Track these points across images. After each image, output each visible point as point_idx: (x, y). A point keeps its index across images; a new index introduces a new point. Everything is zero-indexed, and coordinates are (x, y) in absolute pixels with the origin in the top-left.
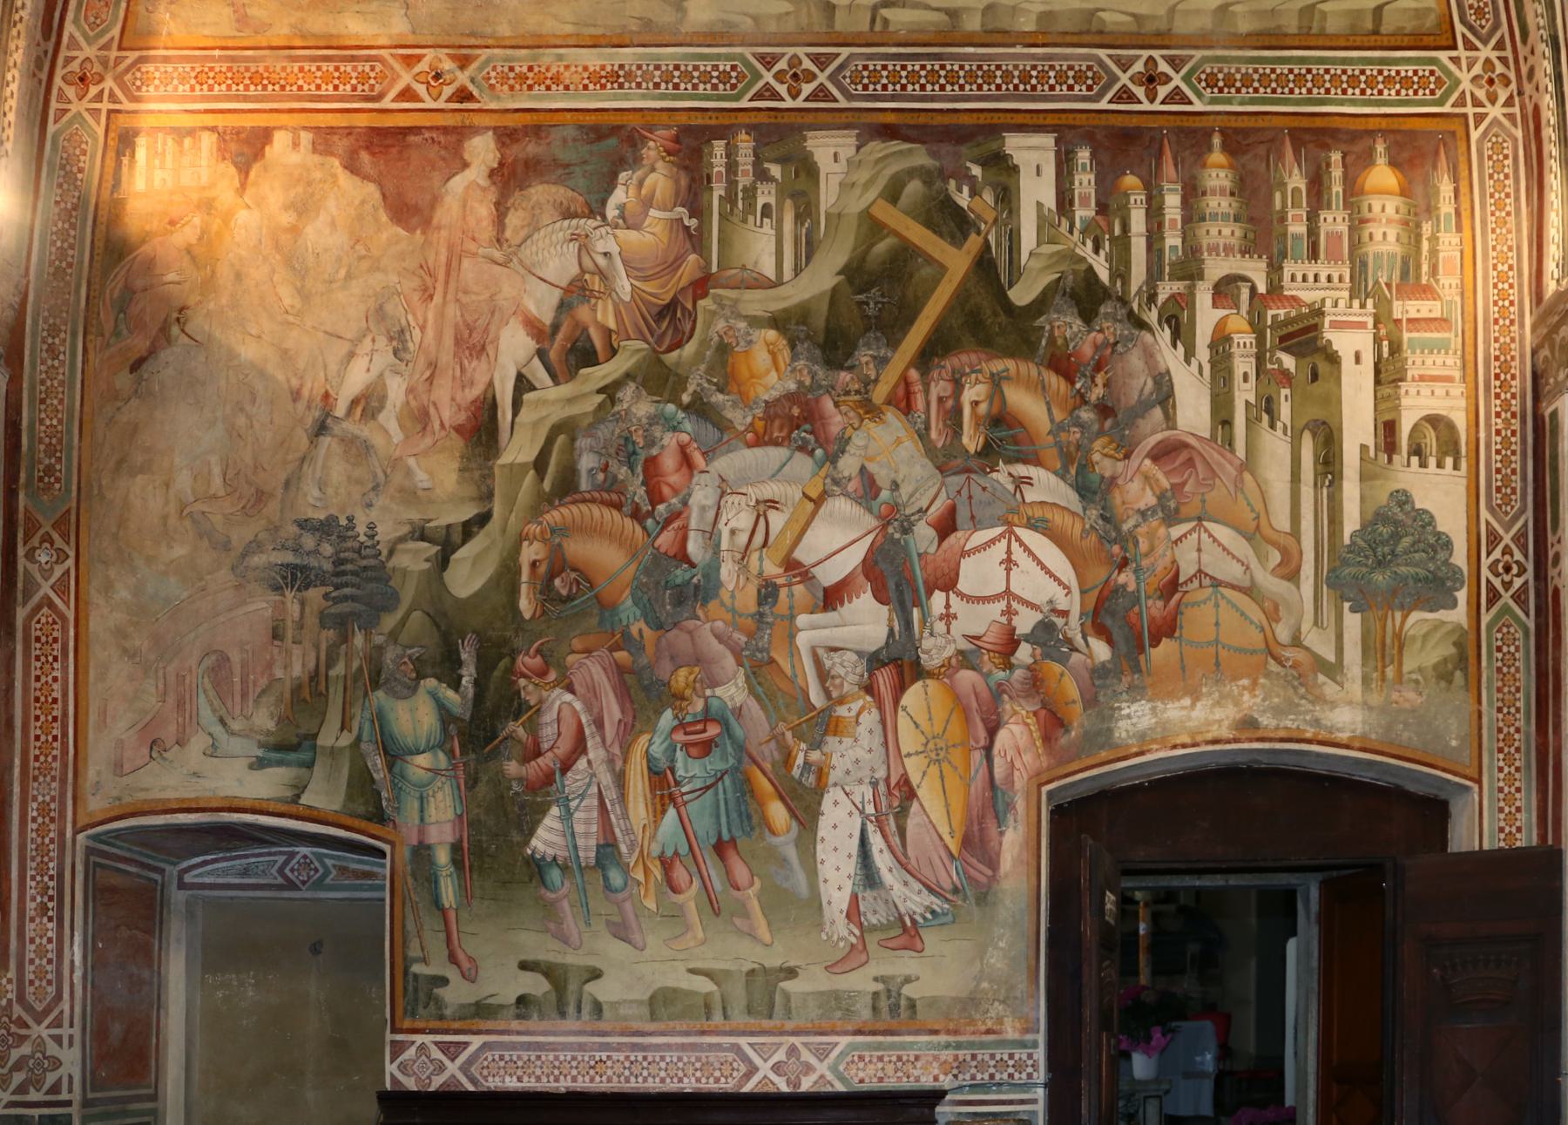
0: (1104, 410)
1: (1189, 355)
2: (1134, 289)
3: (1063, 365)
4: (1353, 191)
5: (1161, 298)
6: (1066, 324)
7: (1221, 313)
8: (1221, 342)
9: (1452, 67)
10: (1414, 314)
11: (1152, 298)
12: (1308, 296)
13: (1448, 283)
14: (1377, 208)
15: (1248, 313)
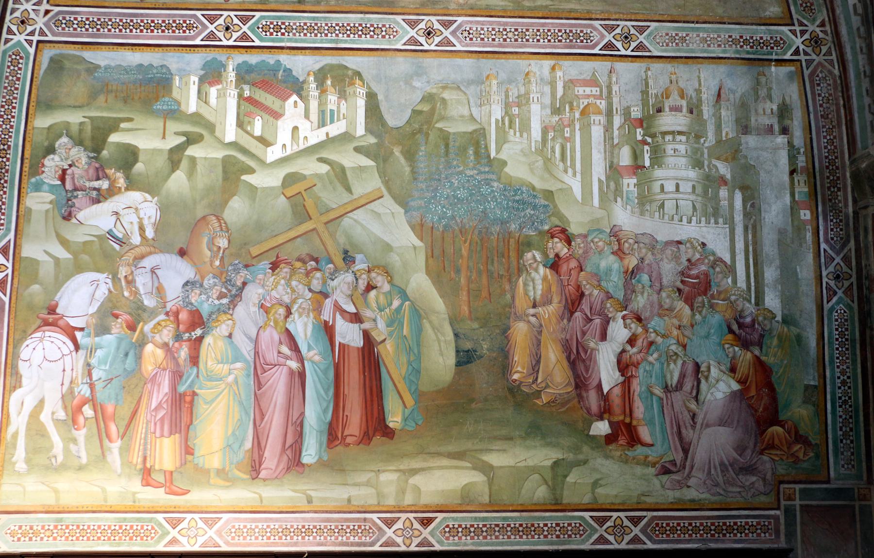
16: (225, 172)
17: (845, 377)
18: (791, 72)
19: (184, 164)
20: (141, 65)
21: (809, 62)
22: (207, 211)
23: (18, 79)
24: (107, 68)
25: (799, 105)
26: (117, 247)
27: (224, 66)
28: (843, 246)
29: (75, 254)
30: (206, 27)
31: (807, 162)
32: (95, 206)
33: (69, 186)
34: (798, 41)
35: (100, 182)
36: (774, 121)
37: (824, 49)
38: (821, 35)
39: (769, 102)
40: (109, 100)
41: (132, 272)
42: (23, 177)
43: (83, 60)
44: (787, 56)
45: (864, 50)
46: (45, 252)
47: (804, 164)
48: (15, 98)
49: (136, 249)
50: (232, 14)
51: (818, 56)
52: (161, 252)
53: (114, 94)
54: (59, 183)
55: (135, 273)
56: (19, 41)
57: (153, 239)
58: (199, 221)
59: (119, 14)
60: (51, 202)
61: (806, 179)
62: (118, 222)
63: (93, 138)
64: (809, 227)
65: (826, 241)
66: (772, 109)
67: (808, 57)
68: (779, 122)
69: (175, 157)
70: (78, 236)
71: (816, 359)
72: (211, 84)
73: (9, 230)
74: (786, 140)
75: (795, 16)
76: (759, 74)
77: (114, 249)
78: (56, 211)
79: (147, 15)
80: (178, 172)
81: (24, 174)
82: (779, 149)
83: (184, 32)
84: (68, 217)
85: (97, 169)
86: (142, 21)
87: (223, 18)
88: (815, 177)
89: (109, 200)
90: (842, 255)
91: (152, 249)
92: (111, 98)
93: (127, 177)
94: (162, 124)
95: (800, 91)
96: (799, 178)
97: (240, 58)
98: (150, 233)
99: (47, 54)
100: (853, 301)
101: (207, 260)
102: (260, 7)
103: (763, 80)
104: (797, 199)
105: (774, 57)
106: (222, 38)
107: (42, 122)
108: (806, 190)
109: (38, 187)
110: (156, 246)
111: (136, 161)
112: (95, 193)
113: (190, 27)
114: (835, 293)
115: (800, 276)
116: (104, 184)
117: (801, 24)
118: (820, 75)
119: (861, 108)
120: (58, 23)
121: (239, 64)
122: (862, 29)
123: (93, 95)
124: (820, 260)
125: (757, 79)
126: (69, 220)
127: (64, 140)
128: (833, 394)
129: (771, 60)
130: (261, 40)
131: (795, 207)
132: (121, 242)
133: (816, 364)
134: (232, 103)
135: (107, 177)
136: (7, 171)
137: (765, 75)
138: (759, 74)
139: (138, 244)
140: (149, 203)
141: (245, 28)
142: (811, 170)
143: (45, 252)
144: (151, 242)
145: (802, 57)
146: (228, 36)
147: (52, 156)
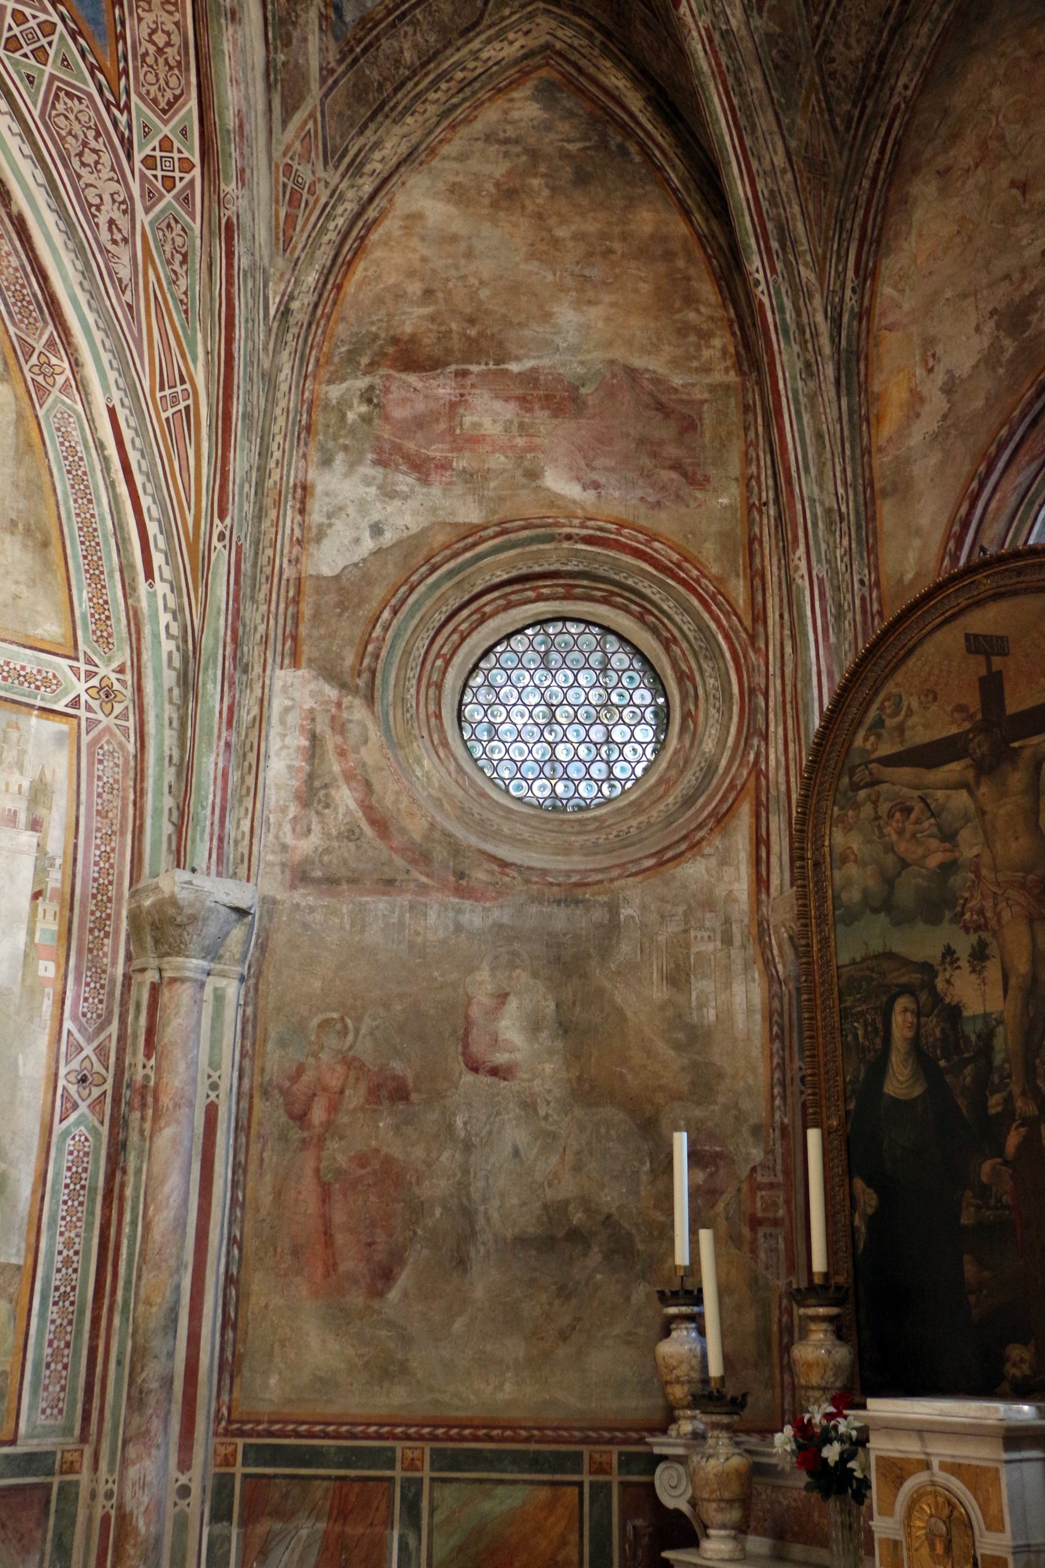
17: (71, 1253)
18: (61, 732)
21: (92, 723)
25: (65, 787)
28: (101, 1028)
31: (63, 882)
34: (80, 687)
36: (21, 807)
37: (118, 708)
38: (117, 686)
39: (17, 773)
44: (60, 707)
45: (175, 724)
47: (58, 885)
51: (107, 716)
61: (57, 909)
64: (49, 990)
65: (74, 1018)
66: (20, 786)
67: (91, 715)
68: (28, 809)
71: (26, 1221)
74: (35, 840)
75: (82, 647)
76: (9, 725)
82: (21, 853)
88: (72, 909)
90: (95, 1044)
95: (70, 765)
96: (47, 907)
100: (102, 1123)
103: (14, 735)
104: (37, 941)
105: (38, 703)
108: (55, 928)
114: (75, 1106)
115: (21, 1073)
117: (89, 661)
118: (106, 747)
119: (157, 812)
122: (176, 692)
124: (59, 1049)
125: (5, 732)
128: (47, 1280)
129: (32, 707)
131: (30, 955)
133: (25, 1227)
137: (18, 728)
138: (9, 725)
142: (68, 897)
145: (82, 713)
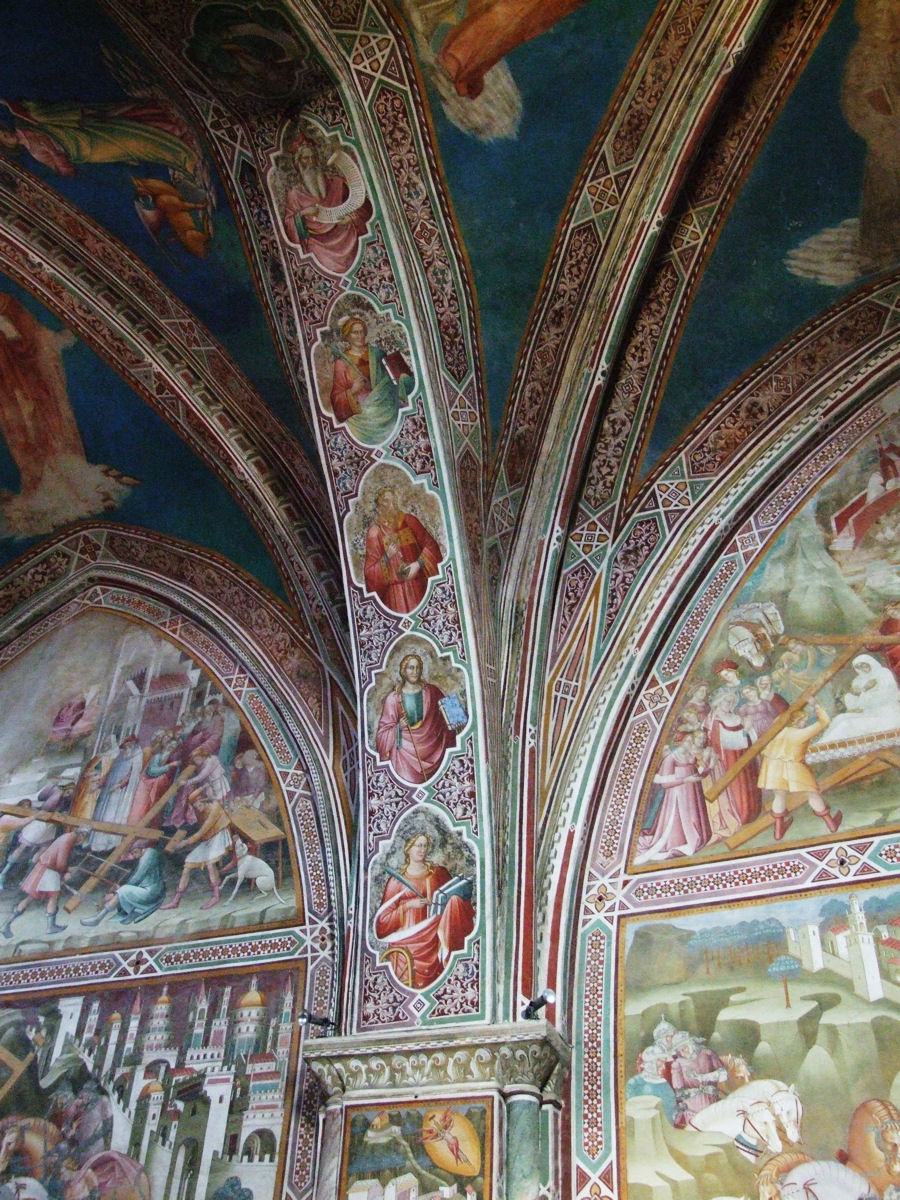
0: (73, 1142)
1: (126, 1105)
2: (104, 1073)
3: (57, 1119)
4: (234, 1005)
5: (117, 1076)
6: (66, 1098)
7: (148, 1081)
8: (145, 1097)
9: (301, 935)
10: (258, 1071)
11: (112, 1077)
12: (198, 1067)
13: (282, 1052)
14: (246, 1013)
15: (164, 1080)
16: (880, 1040)
19: (822, 1036)
20: (743, 924)
22: (867, 1096)
23: (601, 962)
24: (703, 933)
26: (752, 1158)
27: (848, 907)
29: (698, 1174)
30: (816, 866)
32: (714, 1105)
33: (677, 1083)
35: (716, 1073)
40: (712, 971)
41: (778, 1193)
42: (619, 1079)
43: (672, 929)
46: (658, 1174)
48: (600, 985)
49: (779, 1159)
50: (844, 845)
52: (813, 1159)
53: (716, 963)
54: (664, 1080)
55: (782, 1193)
56: (599, 921)
57: (799, 1143)
58: (857, 1110)
59: (708, 870)
60: (656, 1108)
62: (747, 1123)
63: (698, 1019)
69: (808, 1030)
70: (697, 1148)
72: (836, 931)
73: (609, 1149)
77: (749, 1162)
78: (664, 1116)
79: (740, 865)
80: (815, 1047)
81: (619, 1074)
83: (789, 876)
84: (681, 1124)
85: (709, 1058)
86: (736, 873)
87: (833, 852)
89: (730, 1096)
91: (801, 1157)
92: (713, 966)
93: (750, 1063)
94: (782, 990)
97: (865, 895)
98: (793, 1135)
99: (631, 929)
101: (882, 1164)
102: (877, 831)
106: (838, 874)
107: (633, 1008)
109: (638, 1090)
110: (805, 1151)
111: (757, 1040)
112: (710, 1089)
113: (796, 869)
116: (722, 1076)
120: (639, 892)
121: (866, 902)
123: (691, 968)
126: (683, 1128)
127: (664, 1026)
130: (887, 867)
132: (756, 1151)
134: (868, 949)
135: (723, 1065)
136: (599, 1074)
139: (780, 1150)
140: (783, 1094)
141: (864, 858)
143: (658, 1174)
144: (797, 1146)
146: (845, 871)
147: (650, 1049)
